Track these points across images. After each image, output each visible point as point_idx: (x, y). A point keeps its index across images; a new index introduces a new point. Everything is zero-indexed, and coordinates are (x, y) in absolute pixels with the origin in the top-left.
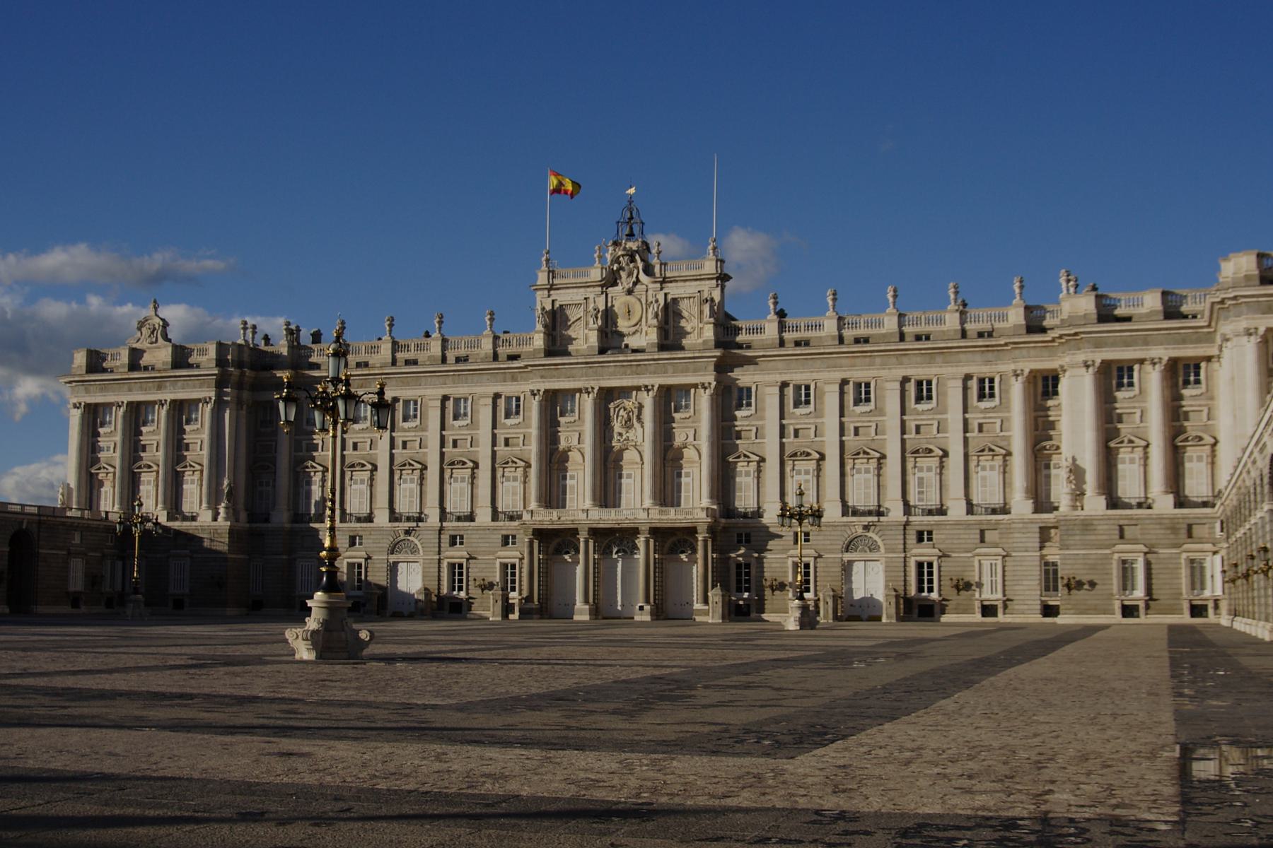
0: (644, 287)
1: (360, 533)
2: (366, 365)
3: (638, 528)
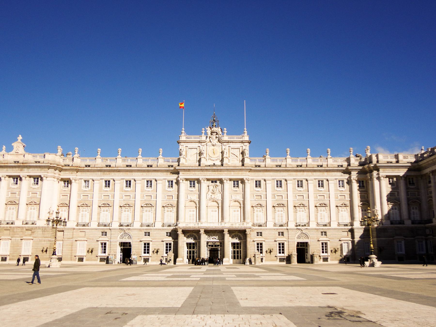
0: (221, 144)
1: (106, 231)
2: (110, 166)
3: (223, 230)
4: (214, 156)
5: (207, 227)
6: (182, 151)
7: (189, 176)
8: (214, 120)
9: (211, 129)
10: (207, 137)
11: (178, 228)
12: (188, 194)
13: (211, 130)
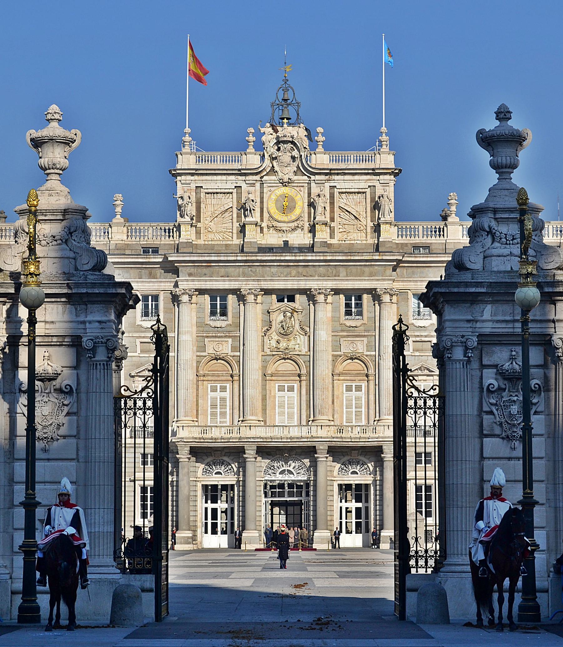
4: (285, 219)
5: (266, 438)
6: (185, 202)
7: (208, 283)
8: (285, 100)
9: (276, 131)
10: (264, 155)
11: (178, 442)
12: (207, 337)
13: (275, 135)
